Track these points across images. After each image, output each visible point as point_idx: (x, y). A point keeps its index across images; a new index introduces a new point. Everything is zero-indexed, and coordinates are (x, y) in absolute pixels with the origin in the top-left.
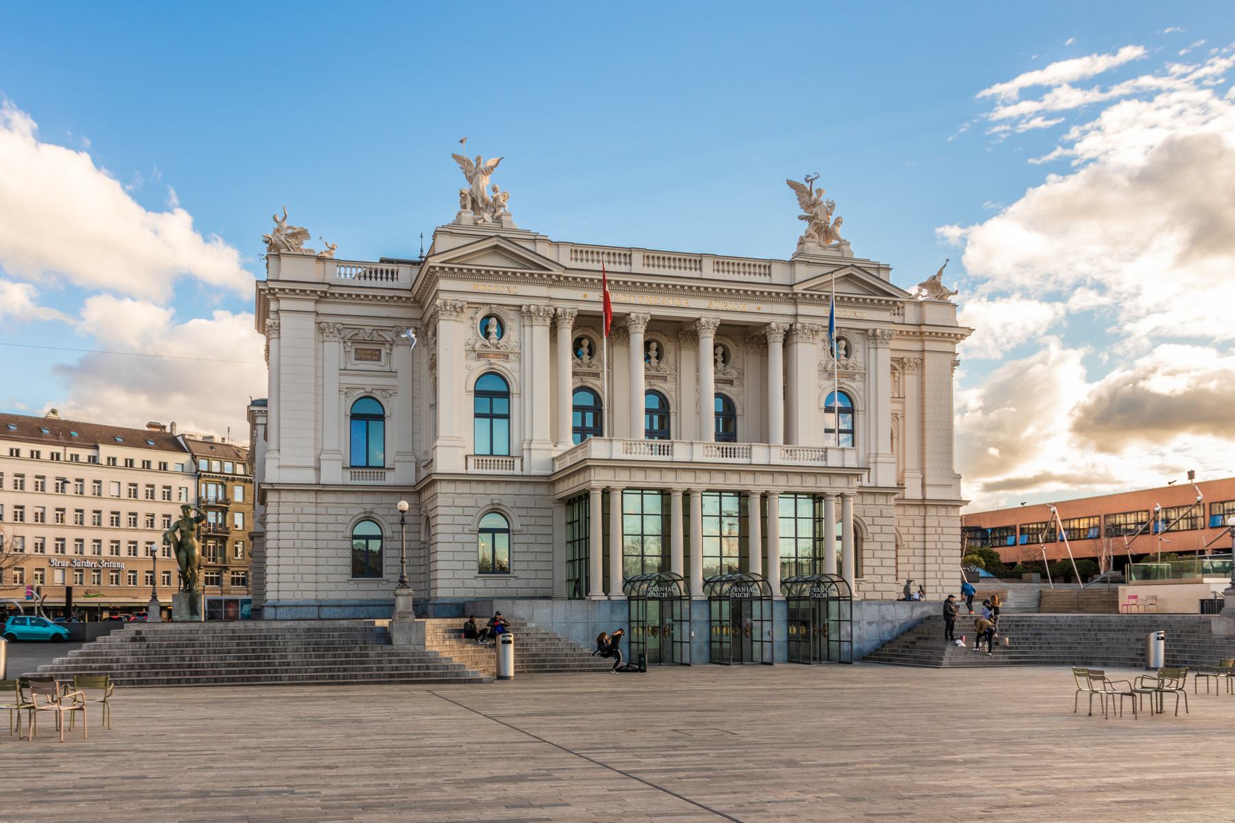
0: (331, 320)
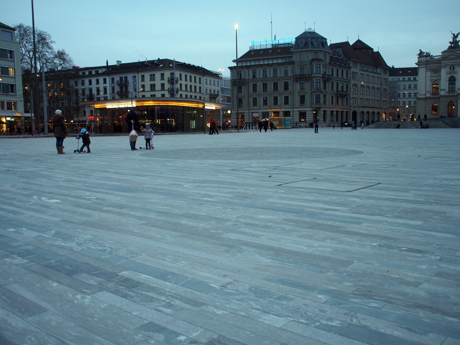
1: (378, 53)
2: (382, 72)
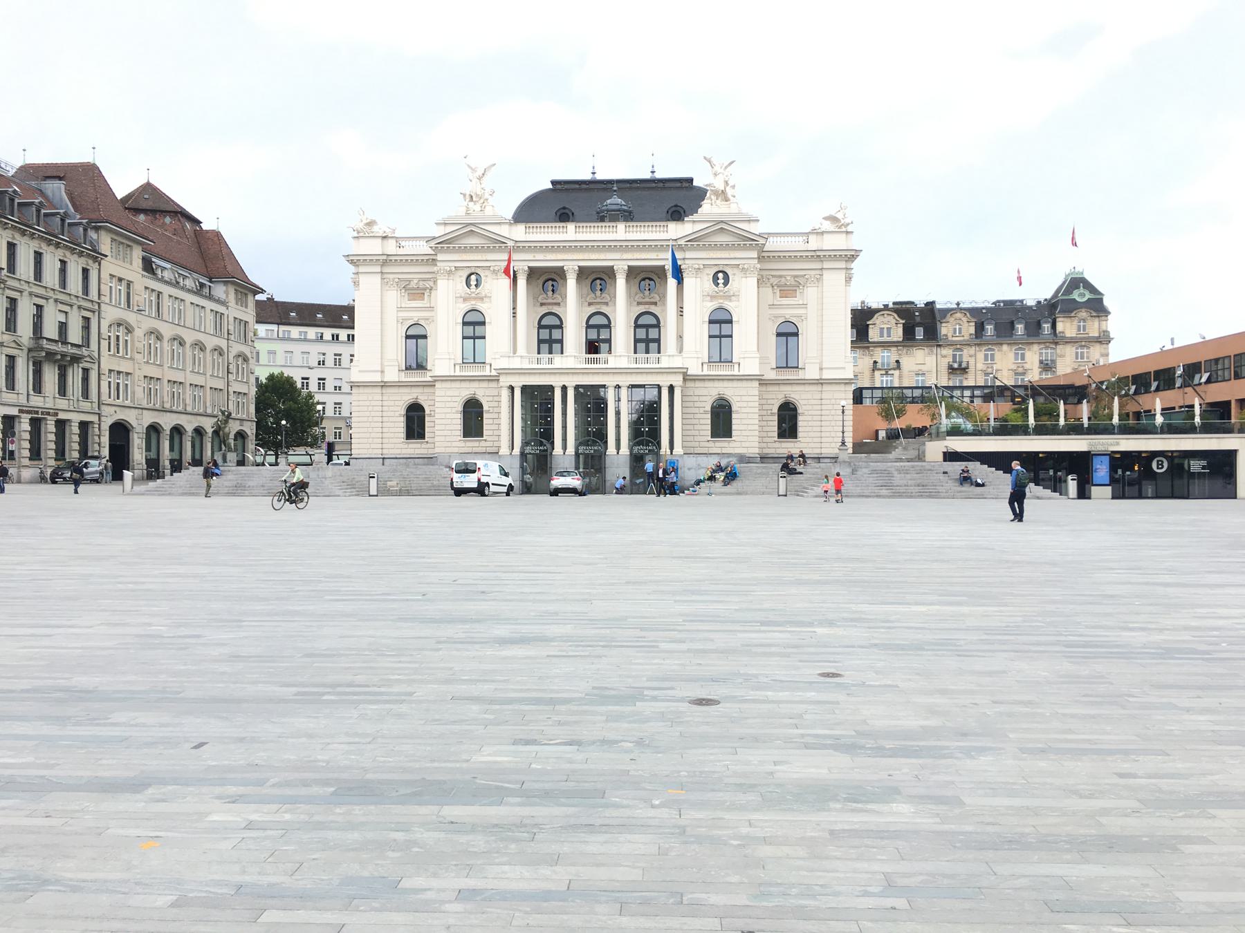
0: (391, 276)
1: (217, 234)
2: (232, 297)
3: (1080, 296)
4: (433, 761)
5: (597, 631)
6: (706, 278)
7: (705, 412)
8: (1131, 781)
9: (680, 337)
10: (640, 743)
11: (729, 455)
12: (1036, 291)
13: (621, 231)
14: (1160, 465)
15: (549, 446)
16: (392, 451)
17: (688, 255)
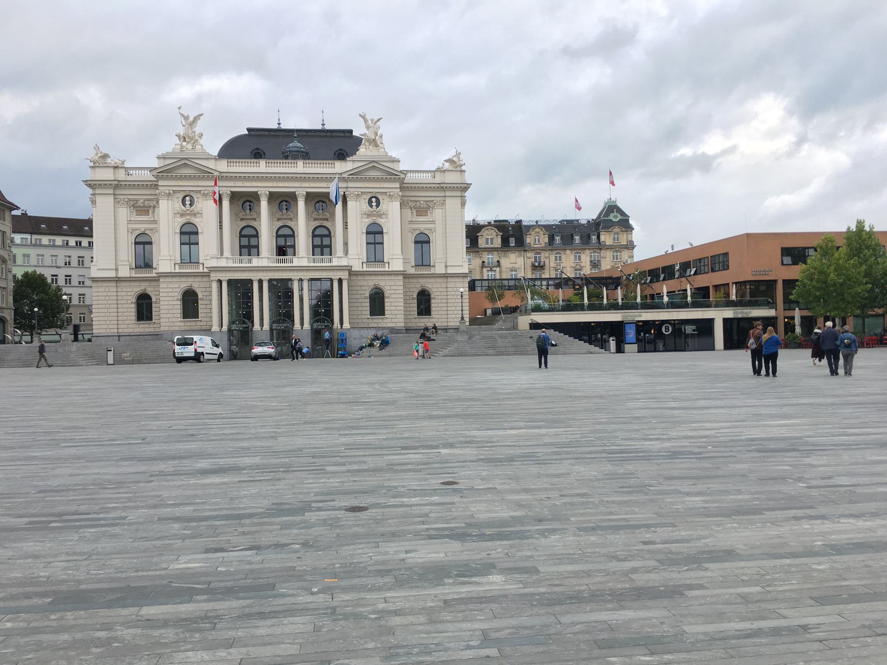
3: (614, 217)
4: (137, 571)
5: (279, 460)
6: (363, 201)
7: (366, 298)
8: (652, 547)
9: (346, 244)
10: (305, 544)
11: (383, 328)
12: (589, 213)
13: (300, 167)
14: (667, 329)
15: (250, 324)
16: (126, 330)
17: (350, 185)
